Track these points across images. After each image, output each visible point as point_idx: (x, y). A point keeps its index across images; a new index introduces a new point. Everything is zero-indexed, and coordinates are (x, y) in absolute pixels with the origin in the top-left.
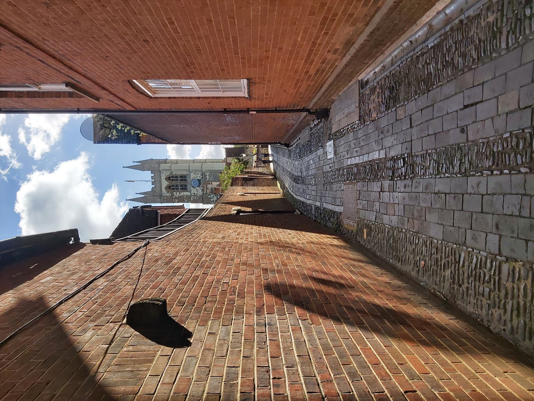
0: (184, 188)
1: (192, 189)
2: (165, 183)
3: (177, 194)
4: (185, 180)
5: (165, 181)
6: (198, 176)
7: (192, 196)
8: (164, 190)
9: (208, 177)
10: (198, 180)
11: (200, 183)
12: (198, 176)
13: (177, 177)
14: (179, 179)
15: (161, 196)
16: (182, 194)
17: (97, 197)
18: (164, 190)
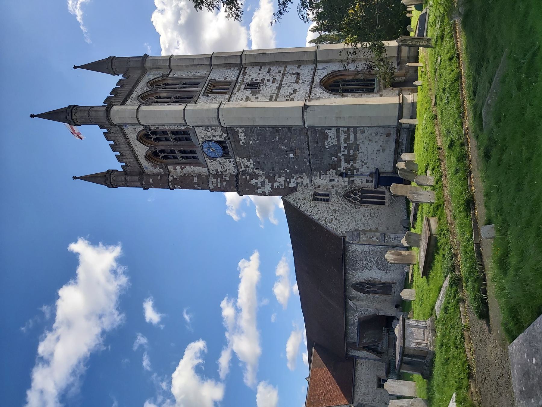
1: (209, 161)
4: (188, 140)
6: (217, 133)
7: (212, 179)
8: (144, 163)
9: (242, 137)
10: (219, 142)
11: (224, 148)
12: (217, 133)
13: (164, 132)
14: (172, 137)
15: (142, 173)
16: (188, 169)
17: (43, 365)
18: (144, 163)
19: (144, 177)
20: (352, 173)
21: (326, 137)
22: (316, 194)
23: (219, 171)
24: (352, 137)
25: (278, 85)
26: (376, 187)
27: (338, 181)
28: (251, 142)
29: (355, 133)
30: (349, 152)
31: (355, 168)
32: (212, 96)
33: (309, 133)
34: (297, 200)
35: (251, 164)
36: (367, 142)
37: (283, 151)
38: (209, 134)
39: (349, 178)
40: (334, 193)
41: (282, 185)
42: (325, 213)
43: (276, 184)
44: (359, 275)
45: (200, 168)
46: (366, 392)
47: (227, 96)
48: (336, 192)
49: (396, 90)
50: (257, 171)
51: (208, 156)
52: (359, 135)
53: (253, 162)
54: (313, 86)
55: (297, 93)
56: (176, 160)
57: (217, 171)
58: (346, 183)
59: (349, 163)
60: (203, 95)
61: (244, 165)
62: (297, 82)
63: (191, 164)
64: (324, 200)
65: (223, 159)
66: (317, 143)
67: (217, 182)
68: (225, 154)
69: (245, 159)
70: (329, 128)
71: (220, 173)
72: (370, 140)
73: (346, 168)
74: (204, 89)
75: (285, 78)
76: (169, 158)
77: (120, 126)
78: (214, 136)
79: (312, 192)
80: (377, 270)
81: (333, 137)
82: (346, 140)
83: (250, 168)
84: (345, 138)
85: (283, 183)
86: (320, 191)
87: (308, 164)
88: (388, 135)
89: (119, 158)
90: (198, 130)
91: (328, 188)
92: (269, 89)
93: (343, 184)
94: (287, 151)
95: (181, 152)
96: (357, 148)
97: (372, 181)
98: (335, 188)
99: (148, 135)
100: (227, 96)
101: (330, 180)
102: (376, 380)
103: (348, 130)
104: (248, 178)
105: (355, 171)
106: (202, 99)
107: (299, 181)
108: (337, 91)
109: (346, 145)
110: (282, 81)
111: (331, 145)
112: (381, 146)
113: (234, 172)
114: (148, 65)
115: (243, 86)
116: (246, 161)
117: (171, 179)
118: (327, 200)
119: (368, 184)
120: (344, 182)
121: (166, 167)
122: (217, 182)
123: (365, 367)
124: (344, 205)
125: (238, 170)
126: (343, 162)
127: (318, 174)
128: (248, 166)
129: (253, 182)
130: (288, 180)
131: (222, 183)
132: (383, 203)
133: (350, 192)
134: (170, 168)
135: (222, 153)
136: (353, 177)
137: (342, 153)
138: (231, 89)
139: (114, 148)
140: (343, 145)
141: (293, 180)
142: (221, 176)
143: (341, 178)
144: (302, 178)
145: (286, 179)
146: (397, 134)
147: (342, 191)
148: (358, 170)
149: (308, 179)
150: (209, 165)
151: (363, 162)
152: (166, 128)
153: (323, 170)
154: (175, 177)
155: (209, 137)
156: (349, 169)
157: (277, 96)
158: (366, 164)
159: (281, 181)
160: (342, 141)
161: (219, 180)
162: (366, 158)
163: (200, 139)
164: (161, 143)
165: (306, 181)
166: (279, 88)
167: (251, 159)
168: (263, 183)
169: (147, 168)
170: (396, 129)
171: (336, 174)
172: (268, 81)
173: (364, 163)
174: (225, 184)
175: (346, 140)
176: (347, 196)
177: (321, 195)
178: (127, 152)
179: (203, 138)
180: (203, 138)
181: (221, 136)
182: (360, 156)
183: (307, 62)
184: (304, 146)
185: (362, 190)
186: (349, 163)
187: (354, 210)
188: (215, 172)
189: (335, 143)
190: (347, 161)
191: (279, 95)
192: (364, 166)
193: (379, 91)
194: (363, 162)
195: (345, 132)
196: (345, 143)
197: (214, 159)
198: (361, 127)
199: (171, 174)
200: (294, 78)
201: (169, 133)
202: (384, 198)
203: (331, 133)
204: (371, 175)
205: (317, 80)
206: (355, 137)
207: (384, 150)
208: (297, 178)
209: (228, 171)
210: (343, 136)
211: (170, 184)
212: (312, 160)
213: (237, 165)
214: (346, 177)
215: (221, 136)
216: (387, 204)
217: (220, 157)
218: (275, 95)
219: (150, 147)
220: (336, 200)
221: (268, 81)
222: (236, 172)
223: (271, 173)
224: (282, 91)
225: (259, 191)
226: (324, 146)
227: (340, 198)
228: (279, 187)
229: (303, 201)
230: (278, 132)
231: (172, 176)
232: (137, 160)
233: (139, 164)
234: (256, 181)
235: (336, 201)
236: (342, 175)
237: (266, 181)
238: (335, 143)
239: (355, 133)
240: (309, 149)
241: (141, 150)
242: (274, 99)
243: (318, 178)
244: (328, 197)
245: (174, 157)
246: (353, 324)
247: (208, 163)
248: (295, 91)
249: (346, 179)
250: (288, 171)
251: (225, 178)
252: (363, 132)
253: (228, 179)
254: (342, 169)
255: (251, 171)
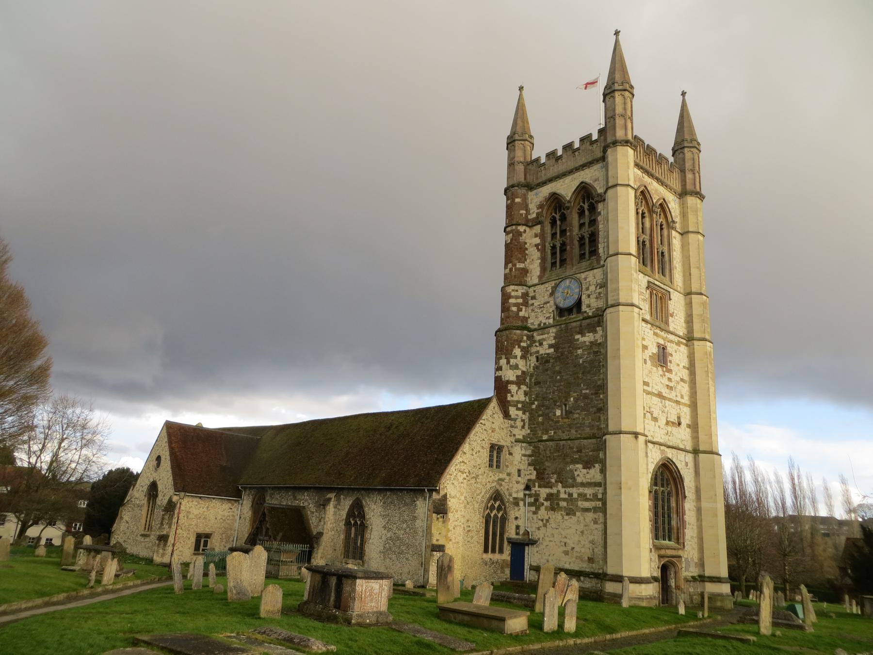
0: (558, 258)
1: (549, 286)
2: (566, 188)
3: (530, 238)
4: (582, 256)
5: (576, 183)
7: (521, 290)
8: (545, 191)
9: (588, 338)
10: (579, 303)
11: (569, 310)
13: (593, 222)
18: (545, 191)
19: (523, 191)
20: (530, 505)
21: (588, 465)
22: (500, 449)
23: (533, 301)
24: (587, 505)
25: (664, 394)
26: (510, 541)
27: (518, 482)
28: (580, 351)
29: (595, 510)
30: (564, 500)
31: (538, 509)
32: (647, 294)
33: (594, 441)
34: (490, 419)
35: (545, 350)
36: (581, 527)
37: (566, 400)
38: (592, 288)
39: (524, 500)
40: (502, 476)
41: (512, 396)
42: (473, 462)
43: (513, 388)
44: (376, 511)
45: (538, 273)
46: (191, 516)
47: (648, 317)
48: (502, 480)
49: (657, 573)
50: (533, 360)
51: (557, 286)
52: (590, 516)
53: (548, 354)
54: (662, 448)
55: (653, 423)
56: (549, 238)
57: (534, 298)
58: (515, 495)
59: (546, 500)
60: (649, 282)
61: (544, 340)
62: (667, 423)
63: (543, 259)
64: (491, 460)
65: (554, 308)
66: (578, 452)
67: (517, 297)
68: (561, 312)
69: (553, 342)
70: (603, 471)
71: (530, 302)
72: (582, 532)
73: (537, 496)
74: (657, 283)
75: (674, 405)
76: (552, 227)
77: (603, 159)
78: (589, 296)
79: (502, 443)
80: (384, 538)
81: (588, 476)
82: (583, 496)
83: (538, 348)
84: (586, 495)
85: (515, 398)
86: (505, 454)
87: (545, 437)
88: (591, 560)
89: (551, 155)
90: (598, 272)
91: (507, 466)
92: (658, 380)
93: (514, 490)
94: (566, 405)
95: (563, 244)
96: (570, 512)
97: (517, 534)
98: (508, 478)
99: (590, 199)
100: (648, 317)
101: (519, 471)
102: (207, 530)
103: (599, 500)
104: (523, 344)
105: (533, 509)
106: (643, 280)
107: (519, 424)
108: (656, 484)
109: (575, 496)
110: (670, 400)
111: (576, 473)
112: (573, 548)
113: (532, 324)
114: (691, 200)
115: (662, 342)
116: (550, 342)
117: (521, 229)
118: (491, 466)
119: (514, 527)
120: (517, 492)
121: (539, 223)
122: (517, 297)
123: (227, 514)
124: (484, 491)
125: (535, 330)
126: (548, 490)
127: (529, 452)
128: (541, 344)
129: (517, 352)
130: (520, 406)
131: (515, 305)
132: (486, 551)
133: (502, 501)
134: (537, 229)
135: (562, 305)
136: (525, 505)
137: (562, 490)
138: (657, 324)
139: (568, 147)
140: (575, 492)
141: (520, 413)
142: (526, 304)
143: (523, 487)
144: (523, 427)
145: (522, 402)
146: (593, 573)
147: (504, 489)
148: (535, 513)
149: (521, 437)
150: (542, 287)
151: (547, 521)
152: (601, 226)
153: (537, 462)
154: (524, 235)
155: (587, 289)
156: (536, 500)
157: (648, 393)
158: (545, 525)
159: (517, 394)
160: (581, 490)
161: (520, 301)
162: (554, 526)
163: (583, 276)
164: (575, 217)
165: (520, 434)
166: (660, 395)
167: (552, 350)
168: (516, 367)
169: (537, 194)
170: (601, 571)
171: (529, 480)
172: (670, 379)
173: (546, 523)
174: (514, 309)
175: (583, 496)
176: (497, 496)
177: (498, 457)
178: (561, 167)
179: (585, 279)
180: (585, 279)
181: (589, 306)
182: (557, 516)
183: (695, 437)
184: (573, 431)
185: (504, 520)
186: (546, 500)
187: (476, 506)
188: (531, 294)
189: (579, 480)
190: (550, 497)
191: (649, 396)
192: (541, 523)
193: (657, 548)
194: (547, 521)
195: (595, 495)
196: (579, 495)
197: (552, 294)
198: (606, 519)
199: (528, 229)
200: (673, 418)
201: (592, 229)
202: (493, 551)
203: (594, 474)
204: (527, 533)
205: (670, 454)
206: (587, 510)
207: (566, 553)
208: (523, 421)
209: (533, 314)
210: (589, 491)
211: (514, 227)
212: (551, 443)
213: (543, 328)
214: (525, 495)
215: (589, 306)
216: (485, 556)
217: (555, 304)
218: (649, 389)
219: (569, 202)
220: (490, 479)
221: (670, 379)
222: (532, 327)
223: (530, 380)
224: (656, 400)
225: (503, 362)
226: (575, 462)
227: (494, 484)
228: (510, 392)
229: (490, 428)
230: (597, 394)
231: (525, 231)
232: (550, 180)
233: (544, 183)
234: (519, 357)
235: (488, 480)
236: (527, 488)
237: (519, 373)
238: (579, 480)
239: (595, 510)
240: (569, 439)
241: (566, 188)
242: (646, 388)
243: (523, 452)
244: (495, 467)
245: (554, 235)
246: (295, 498)
247: (546, 285)
248: (655, 419)
249: (521, 495)
250: (534, 407)
251: (524, 310)
252: (595, 522)
253: (521, 314)
254: (537, 488)
255: (533, 349)
